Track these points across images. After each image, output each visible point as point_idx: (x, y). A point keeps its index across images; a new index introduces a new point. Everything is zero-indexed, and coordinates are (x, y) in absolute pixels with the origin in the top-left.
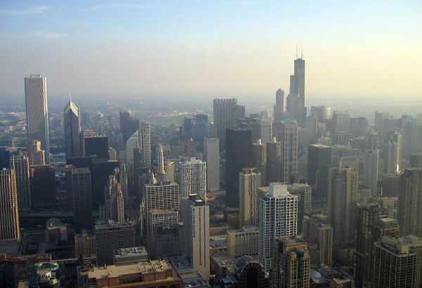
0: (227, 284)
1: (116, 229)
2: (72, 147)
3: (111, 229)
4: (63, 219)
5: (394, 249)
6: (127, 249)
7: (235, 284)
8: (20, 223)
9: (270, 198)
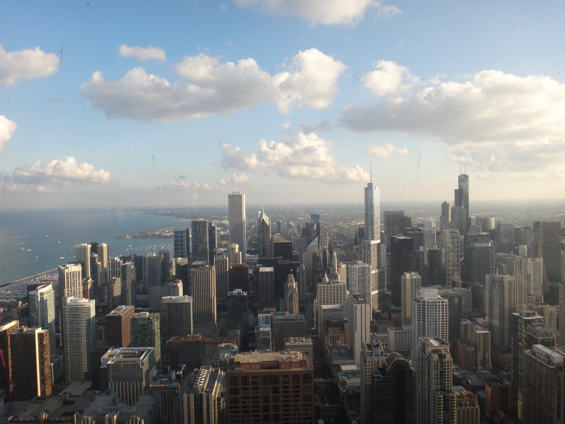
0: (376, 377)
1: (290, 320)
2: (264, 249)
3: (286, 320)
5: (547, 359)
6: (297, 338)
7: (383, 379)
8: (217, 308)
9: (422, 300)
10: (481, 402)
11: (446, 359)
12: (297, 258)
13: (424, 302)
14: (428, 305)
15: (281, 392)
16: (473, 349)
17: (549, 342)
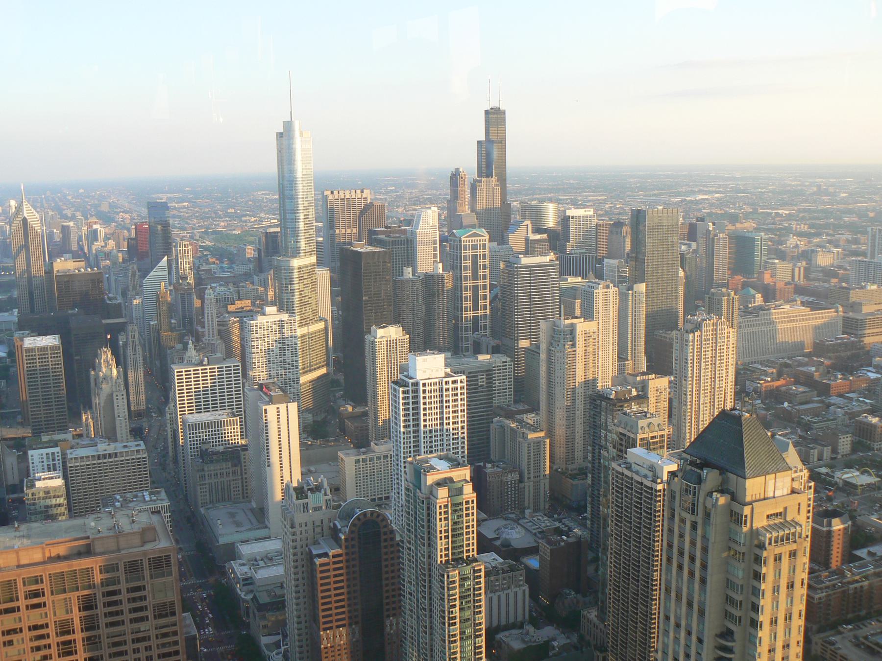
0: (320, 556)
1: (110, 456)
3: (99, 457)
4: (12, 442)
5: (650, 474)
10: (532, 577)
11: (464, 497)
12: (117, 311)
13: (416, 384)
14: (424, 391)
15: (100, 605)
16: (515, 476)
17: (655, 443)
